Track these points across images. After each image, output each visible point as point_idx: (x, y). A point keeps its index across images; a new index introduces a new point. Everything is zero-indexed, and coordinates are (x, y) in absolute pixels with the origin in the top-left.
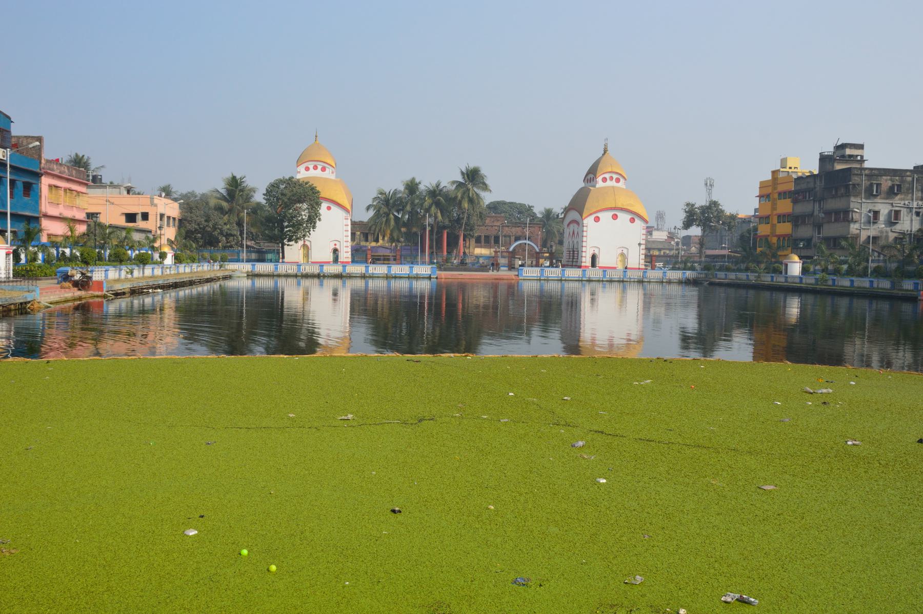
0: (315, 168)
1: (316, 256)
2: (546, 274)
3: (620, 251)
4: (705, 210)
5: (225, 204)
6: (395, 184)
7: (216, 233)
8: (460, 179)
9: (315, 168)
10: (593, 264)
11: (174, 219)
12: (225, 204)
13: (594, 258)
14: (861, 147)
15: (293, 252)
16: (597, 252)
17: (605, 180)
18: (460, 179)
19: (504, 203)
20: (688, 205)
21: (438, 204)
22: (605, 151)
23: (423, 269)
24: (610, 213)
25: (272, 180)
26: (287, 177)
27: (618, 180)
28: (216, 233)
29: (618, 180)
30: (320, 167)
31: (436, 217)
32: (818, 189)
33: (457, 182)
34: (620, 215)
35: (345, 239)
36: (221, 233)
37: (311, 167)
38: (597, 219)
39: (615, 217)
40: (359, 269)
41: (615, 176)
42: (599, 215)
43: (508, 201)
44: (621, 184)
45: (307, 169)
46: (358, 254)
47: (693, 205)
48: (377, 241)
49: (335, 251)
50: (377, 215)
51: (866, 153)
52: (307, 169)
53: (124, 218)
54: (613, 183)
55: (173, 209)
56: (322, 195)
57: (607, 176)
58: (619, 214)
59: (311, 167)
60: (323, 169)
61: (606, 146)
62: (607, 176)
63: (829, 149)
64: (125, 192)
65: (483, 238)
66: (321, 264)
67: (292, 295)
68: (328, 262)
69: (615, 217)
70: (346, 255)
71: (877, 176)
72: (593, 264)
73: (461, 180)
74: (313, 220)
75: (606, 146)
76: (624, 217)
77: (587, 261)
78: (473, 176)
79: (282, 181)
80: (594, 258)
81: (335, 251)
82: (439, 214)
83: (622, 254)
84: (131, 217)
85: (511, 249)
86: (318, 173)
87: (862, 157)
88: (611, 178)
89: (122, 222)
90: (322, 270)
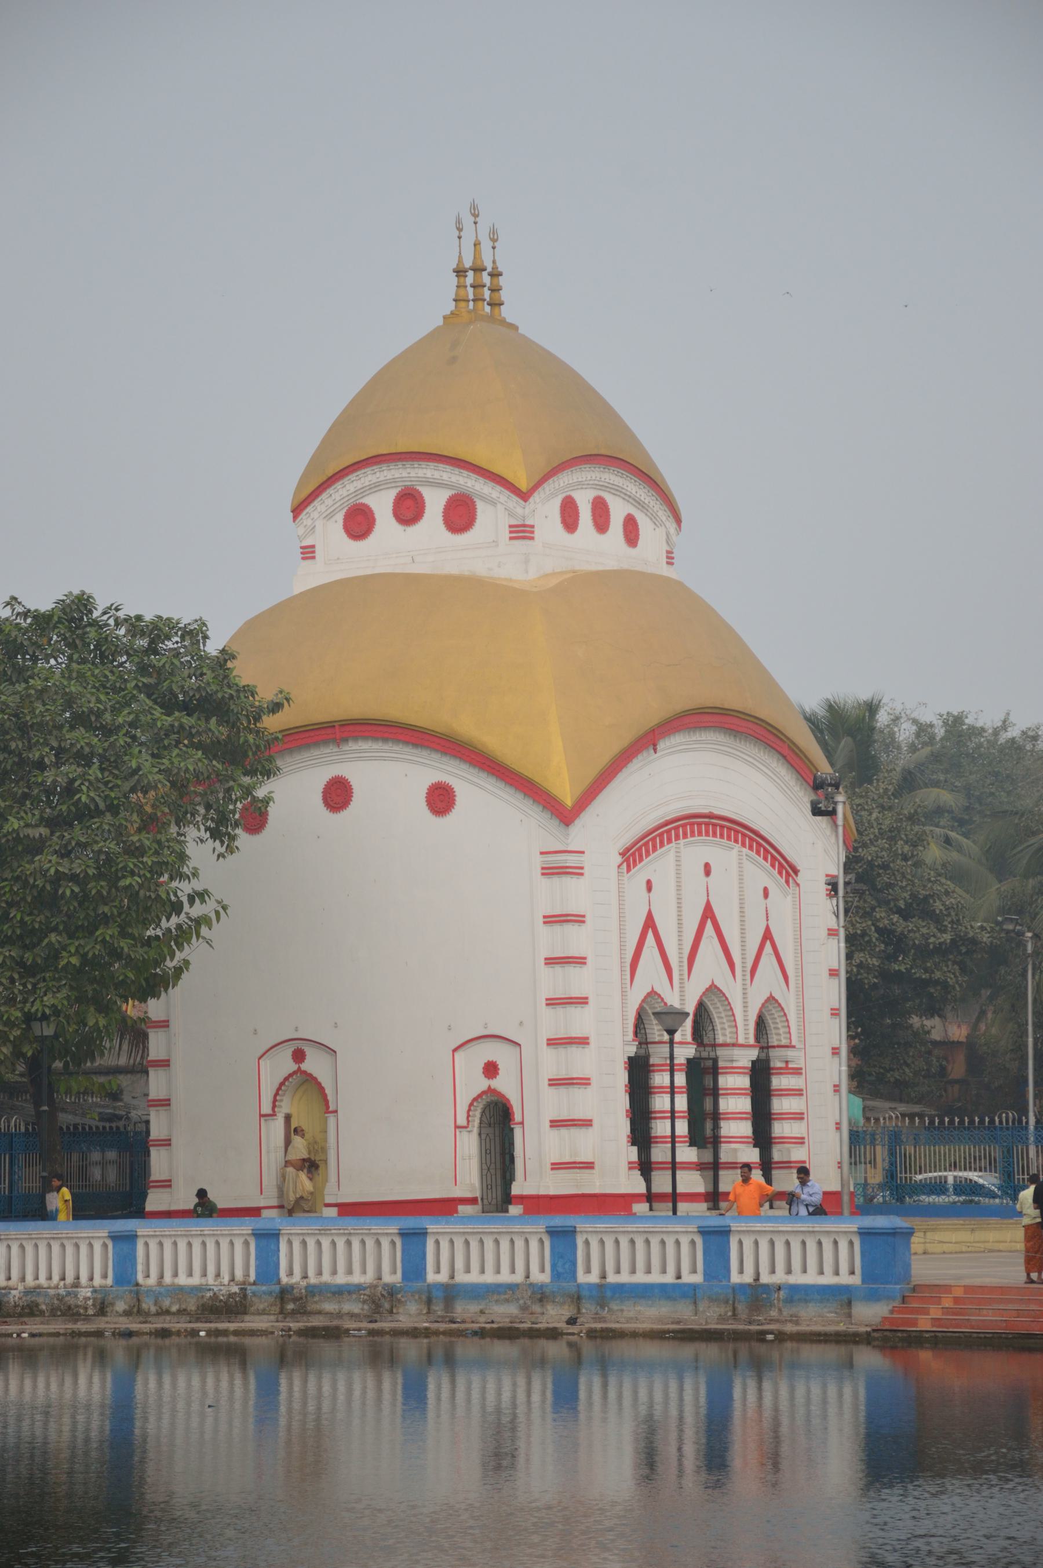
0: (409, 508)
30: (435, 502)
37: (382, 505)
45: (359, 523)
49: (497, 1119)
52: (359, 523)
59: (382, 505)
60: (460, 515)
66: (414, 1215)
68: (445, 1207)
70: (558, 1145)
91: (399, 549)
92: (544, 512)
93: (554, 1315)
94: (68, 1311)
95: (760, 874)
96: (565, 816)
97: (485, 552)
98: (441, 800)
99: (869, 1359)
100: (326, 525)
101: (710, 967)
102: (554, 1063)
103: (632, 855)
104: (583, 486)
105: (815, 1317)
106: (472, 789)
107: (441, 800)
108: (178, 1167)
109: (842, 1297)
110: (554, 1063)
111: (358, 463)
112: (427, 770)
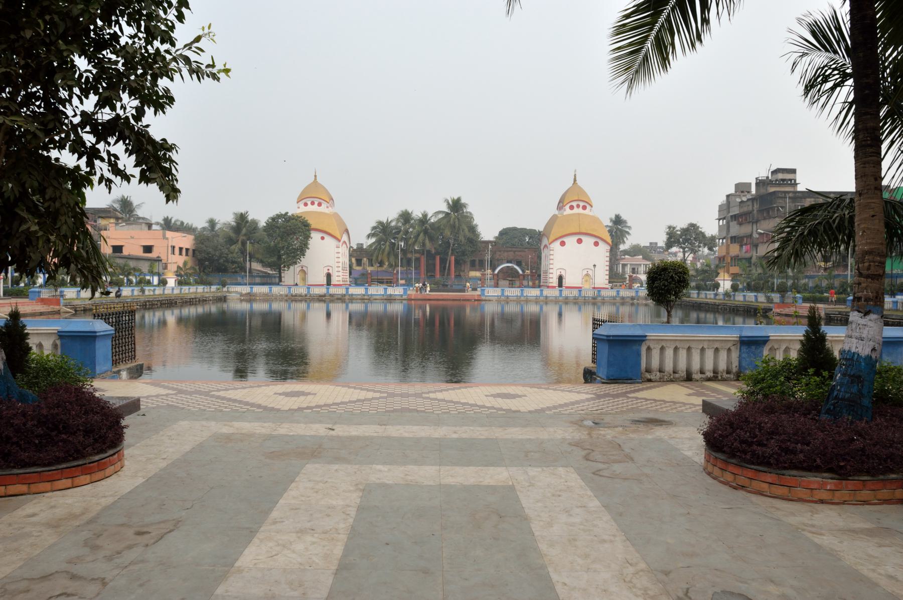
0: (313, 203)
1: (311, 280)
2: (506, 294)
3: (585, 272)
4: (685, 231)
5: (233, 235)
6: (390, 214)
7: (221, 261)
8: (445, 208)
10: (560, 284)
11: (187, 250)
12: (233, 235)
13: (560, 278)
14: (793, 171)
15: (290, 275)
16: (563, 273)
17: (572, 208)
18: (445, 208)
19: (515, 229)
20: (670, 227)
21: (426, 232)
22: (575, 180)
23: (397, 291)
24: (575, 238)
25: (273, 214)
26: (283, 213)
27: (584, 208)
28: (221, 261)
29: (584, 208)
30: (316, 203)
31: (424, 244)
32: (755, 212)
34: (585, 239)
35: (337, 265)
36: (227, 261)
37: (309, 203)
39: (580, 241)
40: (358, 291)
41: (581, 204)
42: (565, 239)
43: (519, 227)
44: (587, 212)
45: (306, 204)
46: (359, 279)
47: (674, 228)
48: (381, 264)
49: (329, 276)
50: (378, 242)
51: (799, 178)
52: (306, 204)
54: (580, 210)
55: (186, 241)
56: (312, 227)
57: (574, 204)
58: (584, 238)
59: (309, 203)
60: (320, 205)
61: (575, 176)
62: (574, 204)
63: (764, 173)
64: (147, 228)
65: (477, 262)
67: (290, 316)
69: (580, 241)
70: (337, 279)
71: (801, 198)
72: (560, 284)
73: (447, 210)
74: (303, 249)
75: (575, 176)
76: (588, 241)
77: (554, 281)
78: (456, 206)
79: (279, 216)
80: (560, 278)
81: (329, 276)
82: (427, 241)
83: (587, 275)
84: (148, 249)
85: (496, 272)
86: (315, 208)
87: (795, 180)
89: (140, 253)
90: (309, 292)
91: (310, 208)
94: (301, 296)
96: (339, 241)
98: (323, 238)
100: (301, 205)
102: (337, 269)
106: (327, 237)
107: (323, 238)
109: (402, 296)
110: (337, 269)
111: (304, 197)
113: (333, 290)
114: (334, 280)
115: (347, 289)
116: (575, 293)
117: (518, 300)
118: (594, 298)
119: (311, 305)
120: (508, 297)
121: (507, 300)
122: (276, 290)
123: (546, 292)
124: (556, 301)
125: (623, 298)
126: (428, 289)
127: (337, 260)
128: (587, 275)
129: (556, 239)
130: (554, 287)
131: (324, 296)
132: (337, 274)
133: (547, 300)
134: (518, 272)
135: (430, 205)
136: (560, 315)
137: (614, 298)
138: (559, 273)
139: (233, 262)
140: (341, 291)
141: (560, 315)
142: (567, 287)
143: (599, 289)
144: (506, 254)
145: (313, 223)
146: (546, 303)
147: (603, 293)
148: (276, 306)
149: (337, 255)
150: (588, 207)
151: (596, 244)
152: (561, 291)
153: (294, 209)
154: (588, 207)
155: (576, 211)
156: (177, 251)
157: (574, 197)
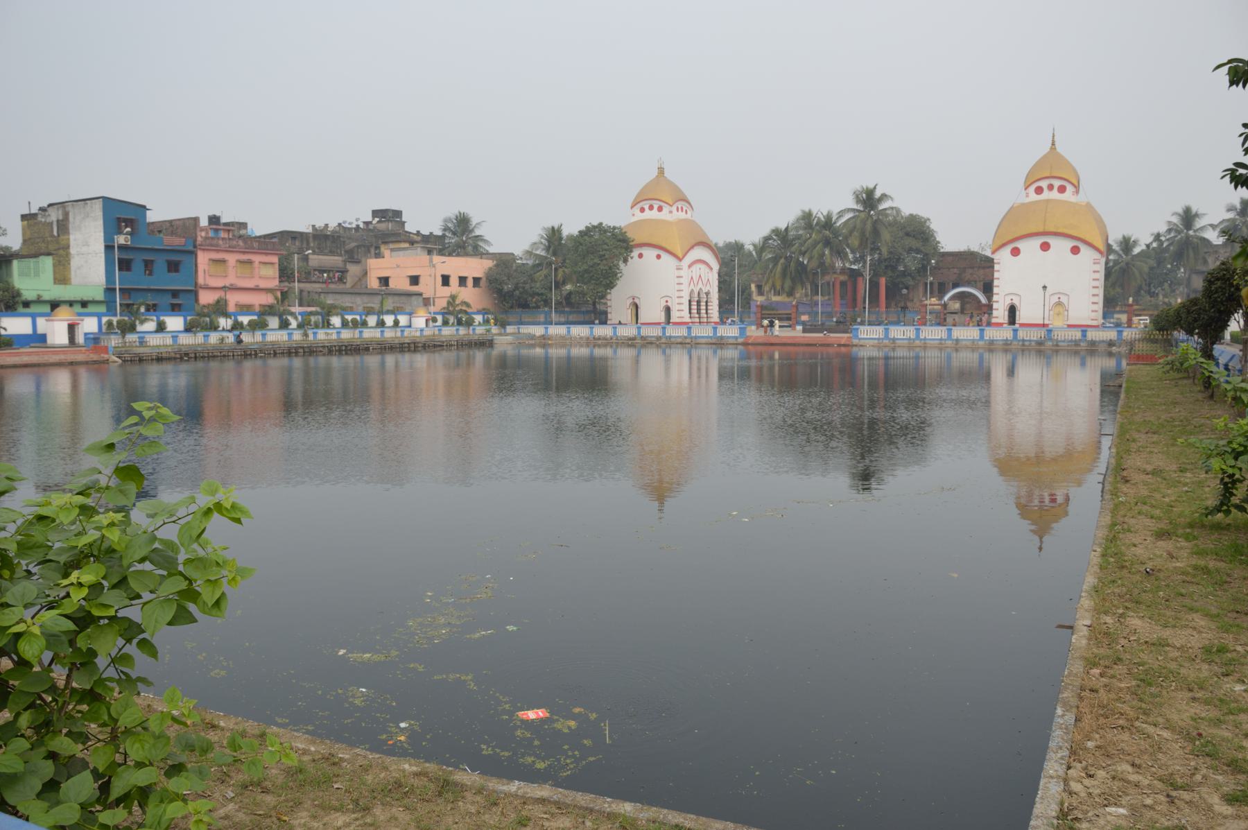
0: (651, 208)
2: (891, 335)
9: (651, 208)
13: (1012, 310)
16: (1016, 302)
24: (1037, 242)
26: (595, 224)
27: (1062, 189)
29: (1062, 189)
30: (656, 207)
33: (853, 210)
35: (677, 294)
37: (646, 207)
38: (1016, 252)
39: (1045, 247)
41: (1057, 183)
44: (1068, 195)
45: (642, 210)
49: (668, 310)
52: (642, 210)
53: (408, 281)
54: (1055, 195)
57: (1044, 184)
58: (1052, 241)
59: (646, 207)
60: (660, 209)
62: (1044, 184)
70: (678, 314)
76: (1061, 246)
77: (1000, 314)
80: (1012, 310)
81: (668, 310)
83: (1059, 304)
84: (415, 280)
86: (654, 214)
88: (1051, 187)
90: (615, 333)
91: (648, 214)
92: (674, 208)
93: (688, 341)
94: (605, 339)
95: (708, 270)
96: (680, 260)
97: (665, 215)
98: (659, 257)
99: (740, 347)
100: (637, 210)
101: (700, 285)
102: (678, 300)
103: (690, 266)
104: (679, 204)
105: (731, 341)
106: (664, 255)
107: (659, 257)
108: (613, 317)
109: (736, 338)
110: (678, 300)
111: (643, 199)
112: (658, 252)
113: (672, 331)
114: (675, 317)
115: (689, 328)
116: (1035, 335)
117: (941, 346)
118: (1040, 343)
119: (619, 351)
120: (894, 340)
121: (958, 345)
122: (601, 331)
123: (991, 333)
124: (1006, 347)
125: (1093, 343)
126: (777, 327)
127: (677, 287)
128: (1059, 304)
129: (1004, 245)
130: (1000, 325)
131: (634, 339)
132: (678, 307)
133: (991, 346)
134: (979, 301)
135: (835, 201)
136: (1011, 372)
137: (1077, 343)
138: (1008, 302)
139: (534, 294)
140: (681, 332)
141: (1011, 372)
142: (1022, 325)
143: (1084, 329)
144: (981, 272)
145: (635, 236)
146: (957, 350)
147: (1092, 335)
148: (598, 352)
149: (677, 280)
150: (1070, 189)
151: (1075, 250)
152: (1015, 331)
153: (618, 216)
154: (1070, 189)
155: (1046, 195)
156: (470, 282)
157: (1051, 172)
